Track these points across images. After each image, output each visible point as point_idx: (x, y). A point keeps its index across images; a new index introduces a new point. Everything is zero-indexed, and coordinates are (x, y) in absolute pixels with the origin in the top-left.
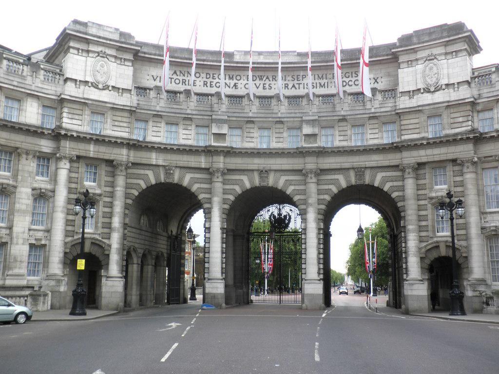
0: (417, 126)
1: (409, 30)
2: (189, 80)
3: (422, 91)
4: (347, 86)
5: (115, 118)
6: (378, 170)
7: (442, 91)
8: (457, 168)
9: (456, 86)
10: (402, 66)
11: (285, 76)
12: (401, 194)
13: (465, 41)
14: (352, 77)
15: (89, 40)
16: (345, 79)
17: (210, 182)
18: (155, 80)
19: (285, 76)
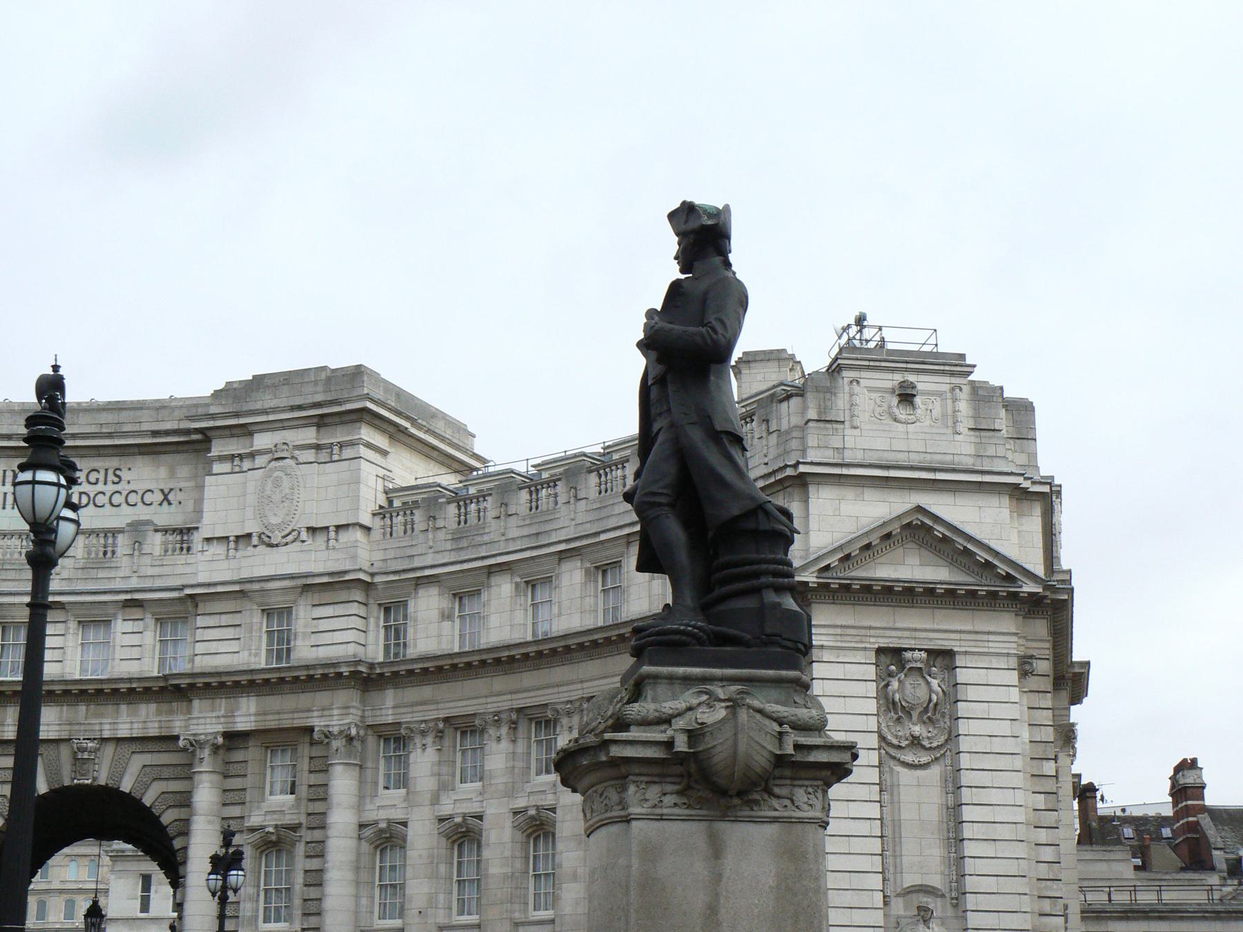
1: (245, 374)
3: (255, 540)
4: (91, 505)
6: (134, 747)
7: (300, 544)
8: (317, 751)
9: (332, 534)
13: (360, 420)
14: (105, 484)
16: (85, 487)
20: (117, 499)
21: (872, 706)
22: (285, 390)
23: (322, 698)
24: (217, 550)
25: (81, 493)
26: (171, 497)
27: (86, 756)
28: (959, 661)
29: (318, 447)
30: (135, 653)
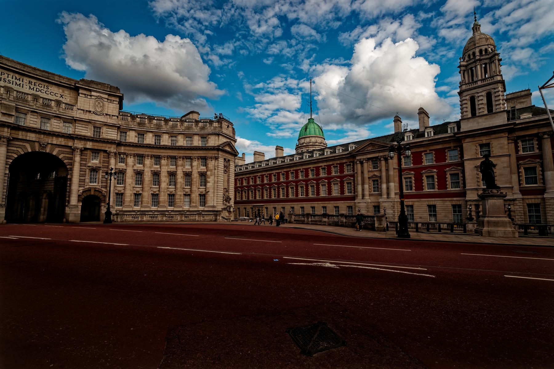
0: (87, 129)
3: (92, 112)
4: (40, 92)
8: (105, 154)
9: (111, 116)
10: (80, 95)
12: (70, 161)
14: (44, 88)
20: (47, 92)
21: (223, 165)
22: (100, 86)
23: (109, 145)
24: (80, 111)
25: (37, 88)
26: (63, 96)
27: (44, 146)
28: (230, 161)
29: (108, 99)
30: (58, 127)
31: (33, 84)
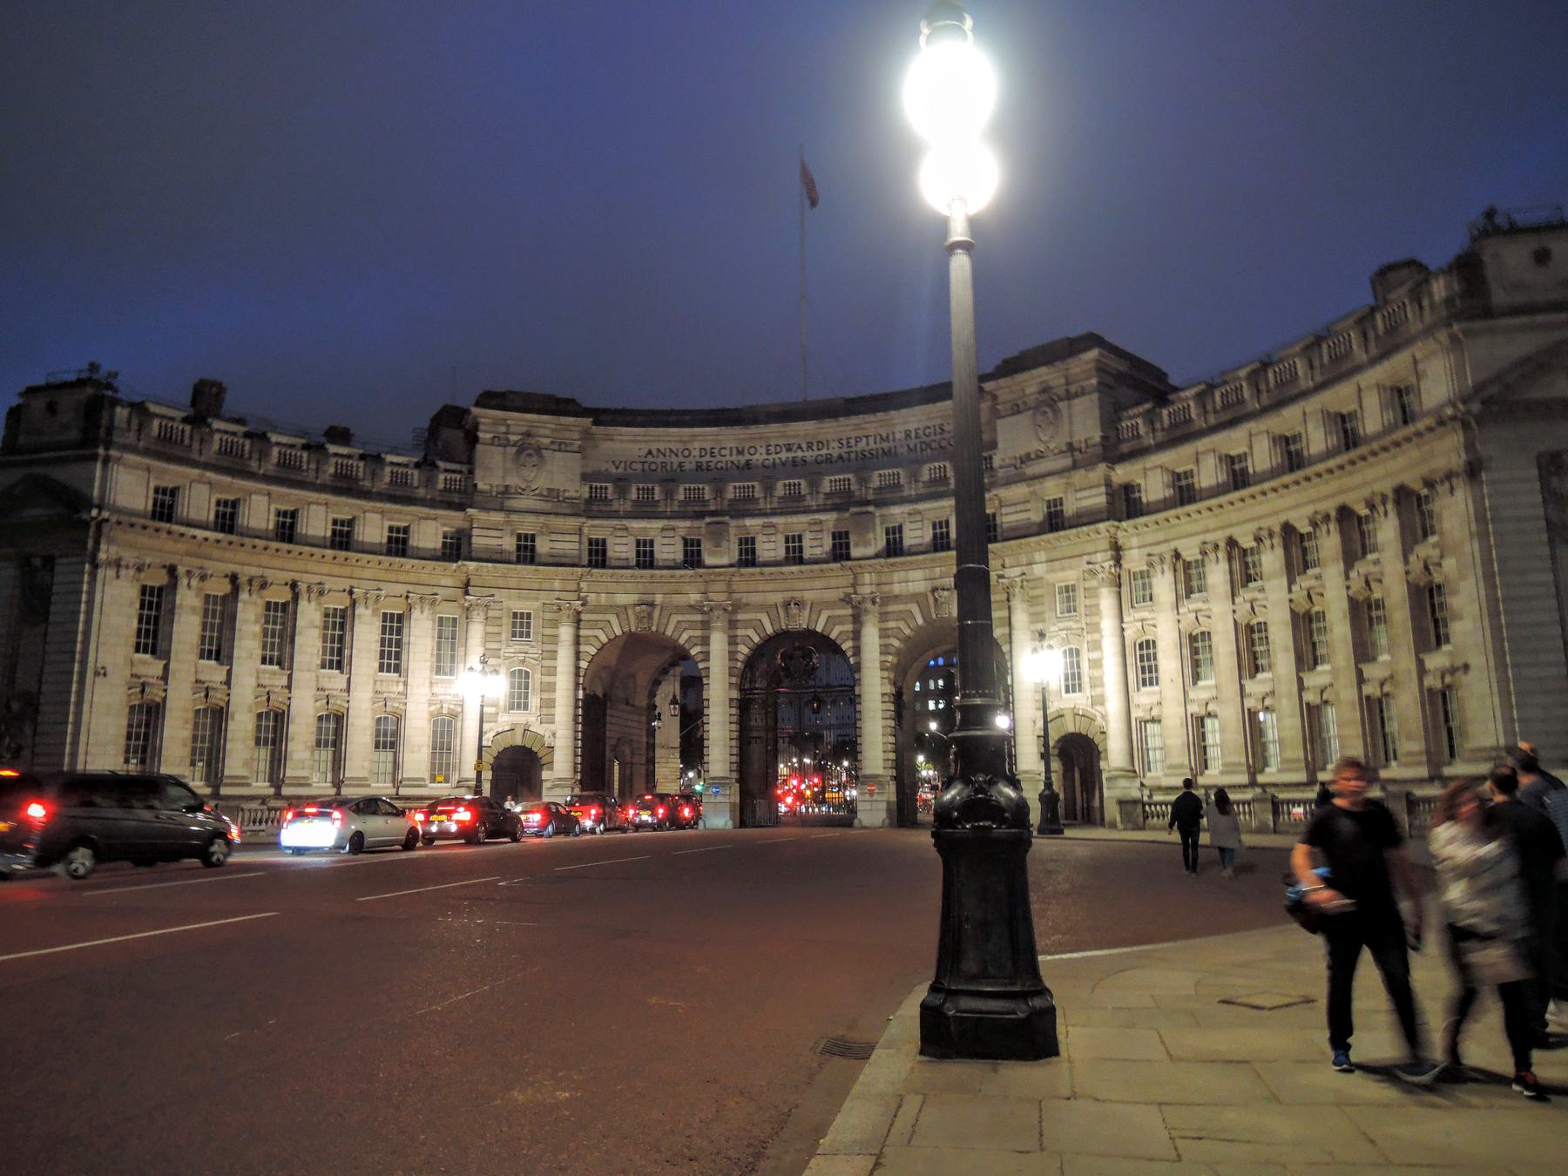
2: (672, 463)
5: (554, 537)
11: (828, 441)
15: (509, 422)
17: (706, 625)
18: (617, 468)
19: (828, 441)
27: (943, 600)
31: (913, 435)
